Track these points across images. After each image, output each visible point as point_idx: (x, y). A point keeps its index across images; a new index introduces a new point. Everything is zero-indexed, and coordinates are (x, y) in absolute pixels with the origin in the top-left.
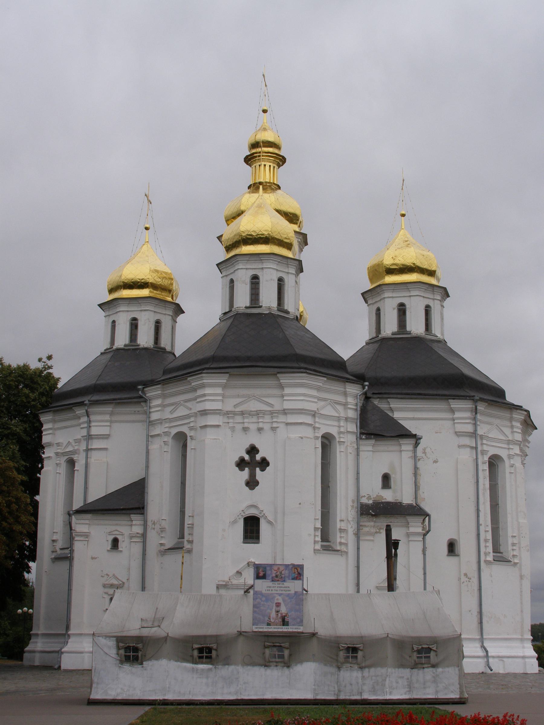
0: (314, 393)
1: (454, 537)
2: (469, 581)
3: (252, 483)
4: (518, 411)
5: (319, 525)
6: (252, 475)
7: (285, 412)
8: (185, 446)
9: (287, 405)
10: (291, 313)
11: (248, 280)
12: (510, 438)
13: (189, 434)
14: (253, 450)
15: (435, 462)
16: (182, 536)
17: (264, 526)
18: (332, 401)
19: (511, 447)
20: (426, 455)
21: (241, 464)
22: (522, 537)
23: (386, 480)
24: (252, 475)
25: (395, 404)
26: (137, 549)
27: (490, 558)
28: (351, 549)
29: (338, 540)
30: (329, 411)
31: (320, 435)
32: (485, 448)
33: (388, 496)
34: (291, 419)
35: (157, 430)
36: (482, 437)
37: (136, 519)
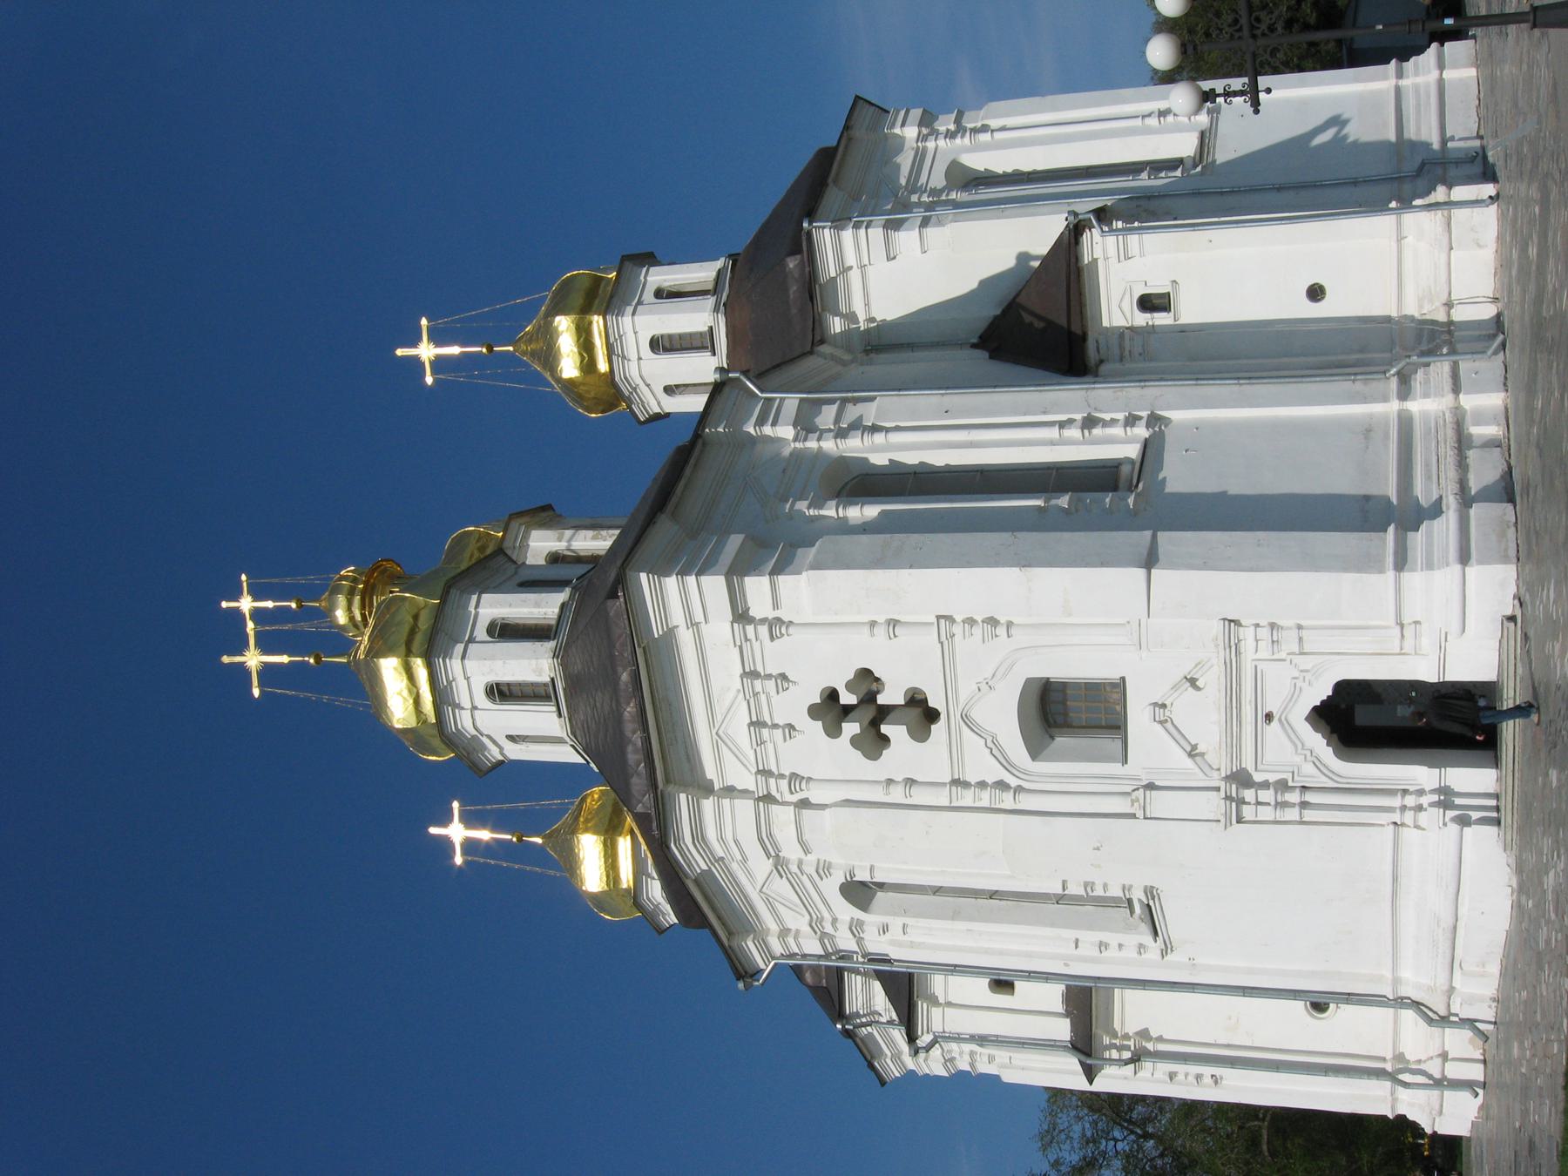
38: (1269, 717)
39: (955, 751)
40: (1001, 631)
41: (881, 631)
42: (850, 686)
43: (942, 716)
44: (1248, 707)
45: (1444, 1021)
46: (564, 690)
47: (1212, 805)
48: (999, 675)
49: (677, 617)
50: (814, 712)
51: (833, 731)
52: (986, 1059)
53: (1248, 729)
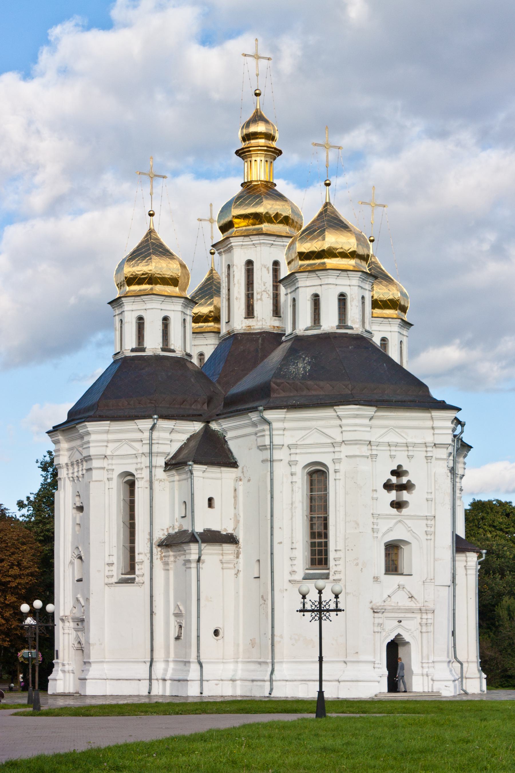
0: (104, 437)
2: (265, 604)
4: (341, 407)
10: (146, 350)
12: (339, 439)
15: (249, 480)
18: (127, 440)
19: (337, 449)
20: (243, 475)
22: (348, 550)
27: (299, 576)
28: (146, 579)
29: (137, 572)
30: (126, 450)
31: (115, 475)
32: (293, 458)
36: (289, 447)
38: (400, 622)
39: (388, 517)
40: (429, 537)
41: (429, 497)
42: (409, 481)
43: (399, 513)
44: (403, 615)
45: (271, 681)
46: (347, 334)
47: (378, 602)
48: (415, 535)
49: (437, 424)
50: (399, 466)
51: (394, 473)
52: (110, 476)
53: (396, 615)
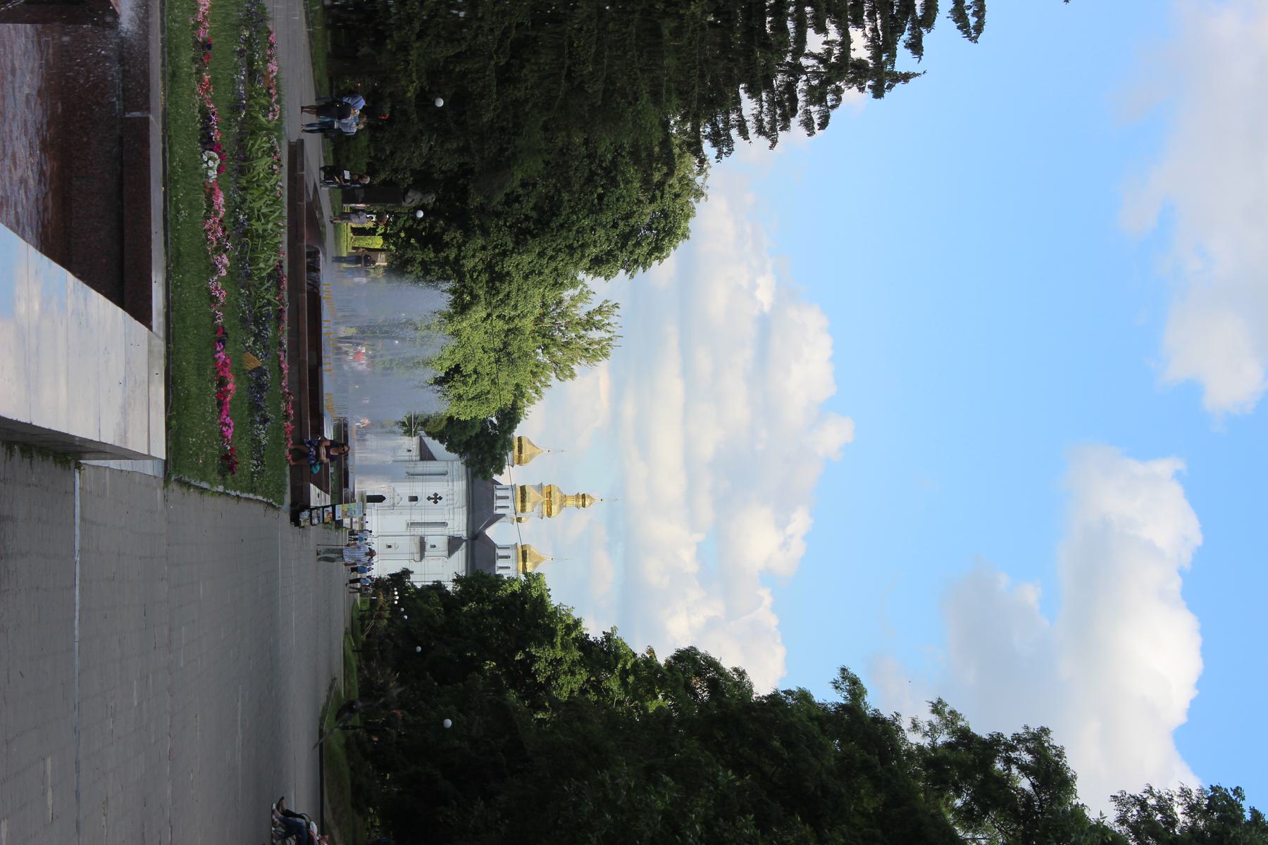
1: (415, 573)
3: (429, 498)
5: (416, 521)
6: (432, 499)
7: (454, 508)
8: (444, 475)
9: (456, 509)
11: (507, 495)
13: (446, 477)
14: (440, 498)
16: (412, 475)
17: (414, 503)
21: (436, 495)
23: (434, 546)
24: (432, 499)
25: (464, 551)
26: (407, 458)
33: (428, 547)
34: (451, 511)
35: (450, 464)
37: (418, 458)
